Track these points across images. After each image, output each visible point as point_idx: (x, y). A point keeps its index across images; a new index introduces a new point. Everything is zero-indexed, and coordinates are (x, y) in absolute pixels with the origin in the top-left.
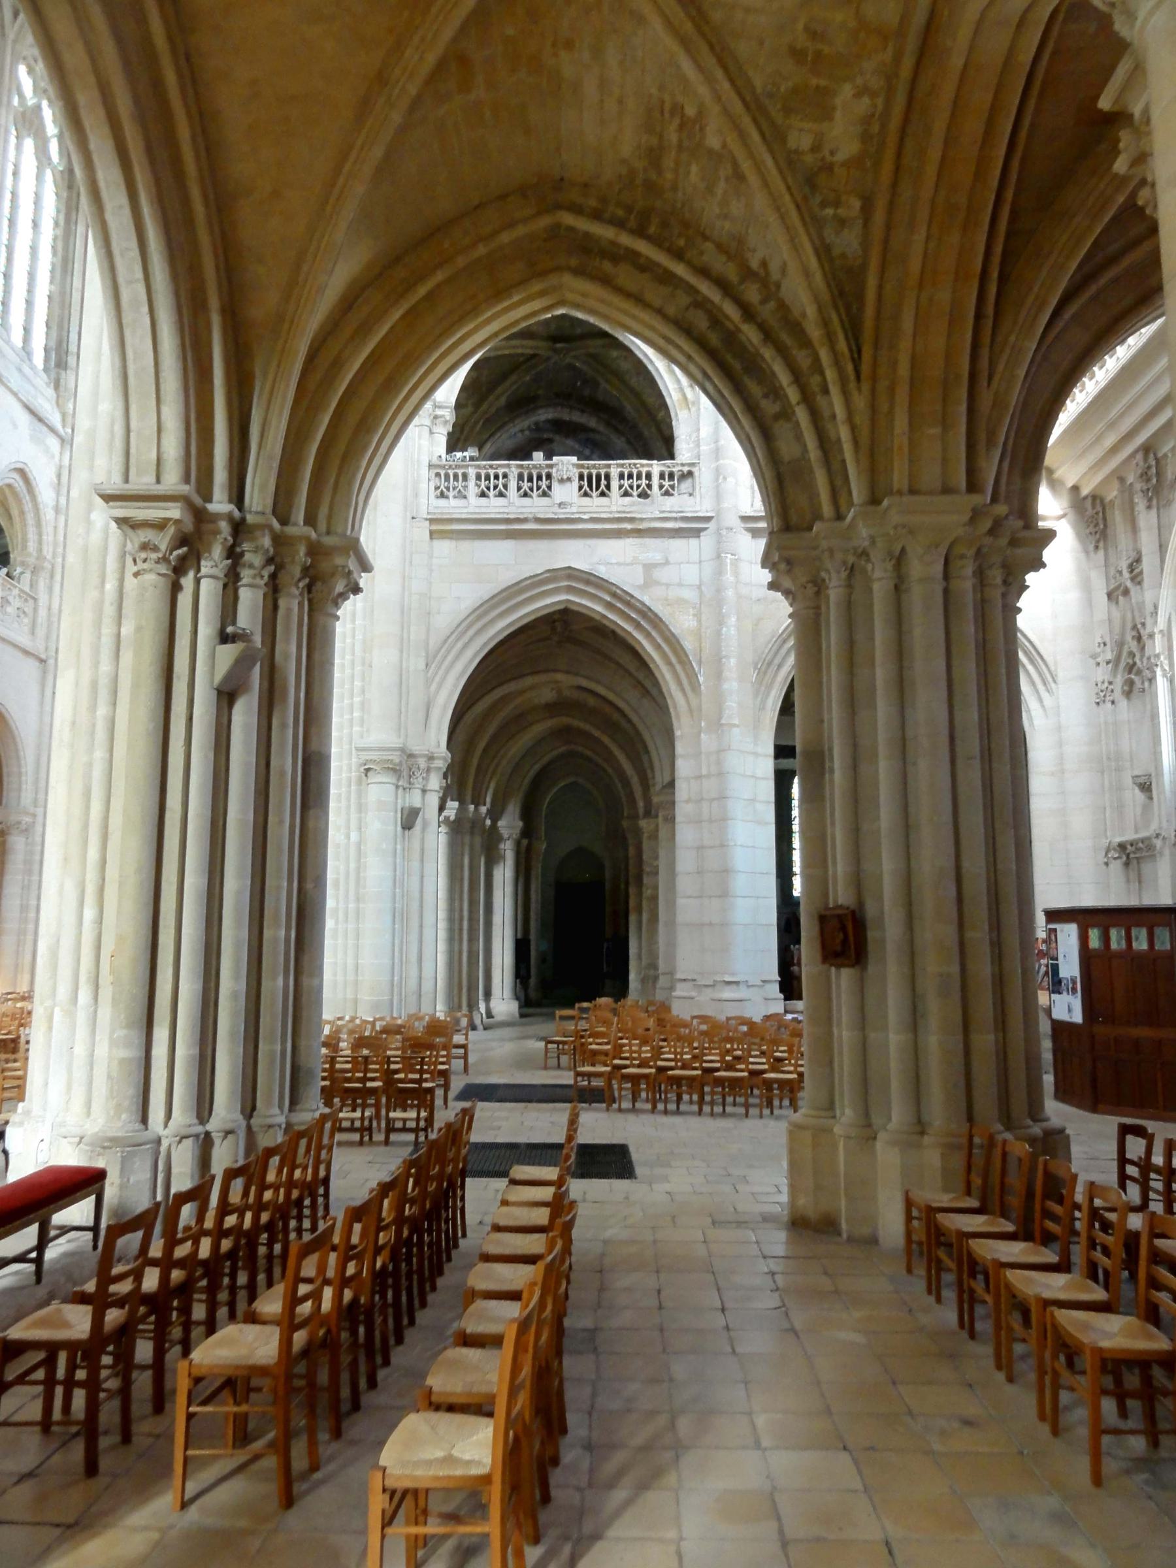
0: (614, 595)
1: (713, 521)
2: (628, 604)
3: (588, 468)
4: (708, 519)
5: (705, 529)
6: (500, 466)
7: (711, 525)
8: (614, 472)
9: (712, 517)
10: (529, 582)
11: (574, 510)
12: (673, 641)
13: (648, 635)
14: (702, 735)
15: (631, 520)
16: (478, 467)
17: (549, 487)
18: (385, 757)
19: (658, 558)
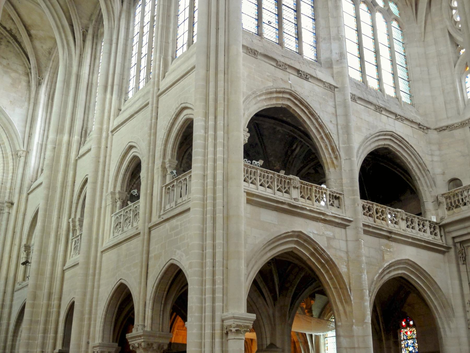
0: (315, 249)
1: (353, 222)
2: (321, 255)
3: (304, 184)
4: (350, 221)
5: (348, 226)
6: (270, 173)
7: (352, 225)
8: (314, 188)
9: (353, 221)
10: (284, 235)
11: (300, 203)
12: (338, 276)
13: (327, 272)
14: (354, 326)
15: (324, 214)
16: (262, 171)
17: (289, 188)
18: (246, 324)
19: (332, 235)
